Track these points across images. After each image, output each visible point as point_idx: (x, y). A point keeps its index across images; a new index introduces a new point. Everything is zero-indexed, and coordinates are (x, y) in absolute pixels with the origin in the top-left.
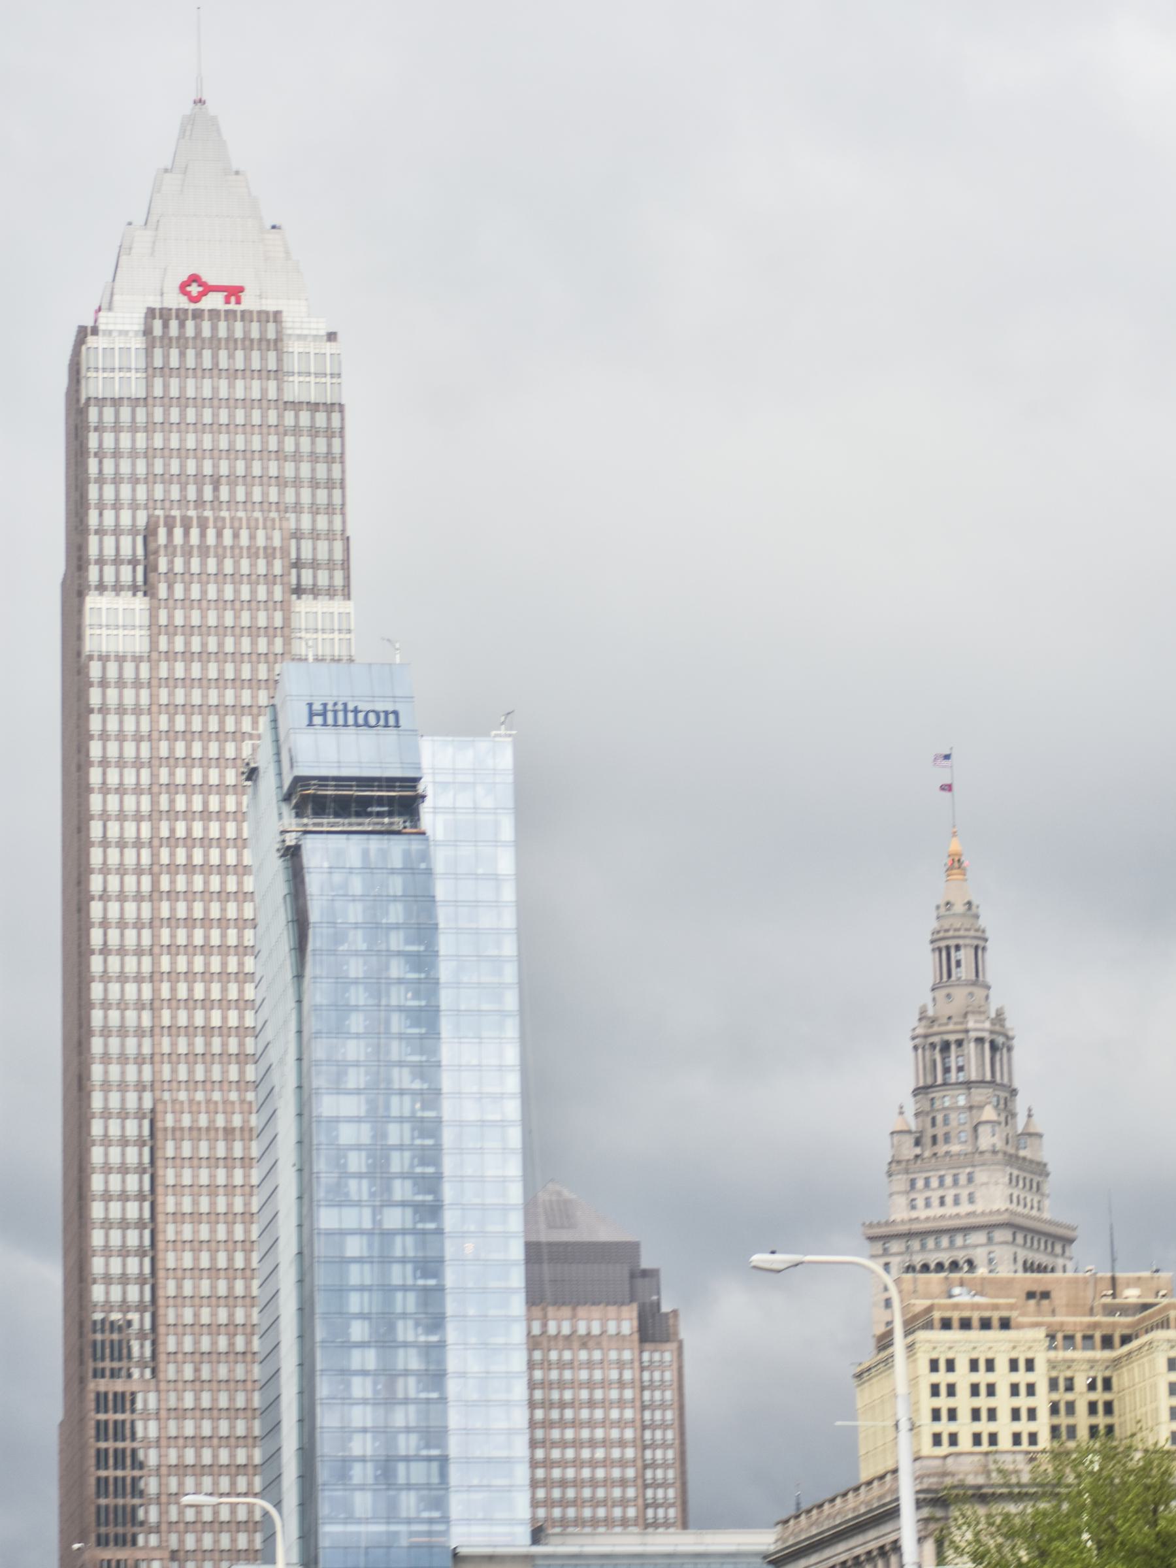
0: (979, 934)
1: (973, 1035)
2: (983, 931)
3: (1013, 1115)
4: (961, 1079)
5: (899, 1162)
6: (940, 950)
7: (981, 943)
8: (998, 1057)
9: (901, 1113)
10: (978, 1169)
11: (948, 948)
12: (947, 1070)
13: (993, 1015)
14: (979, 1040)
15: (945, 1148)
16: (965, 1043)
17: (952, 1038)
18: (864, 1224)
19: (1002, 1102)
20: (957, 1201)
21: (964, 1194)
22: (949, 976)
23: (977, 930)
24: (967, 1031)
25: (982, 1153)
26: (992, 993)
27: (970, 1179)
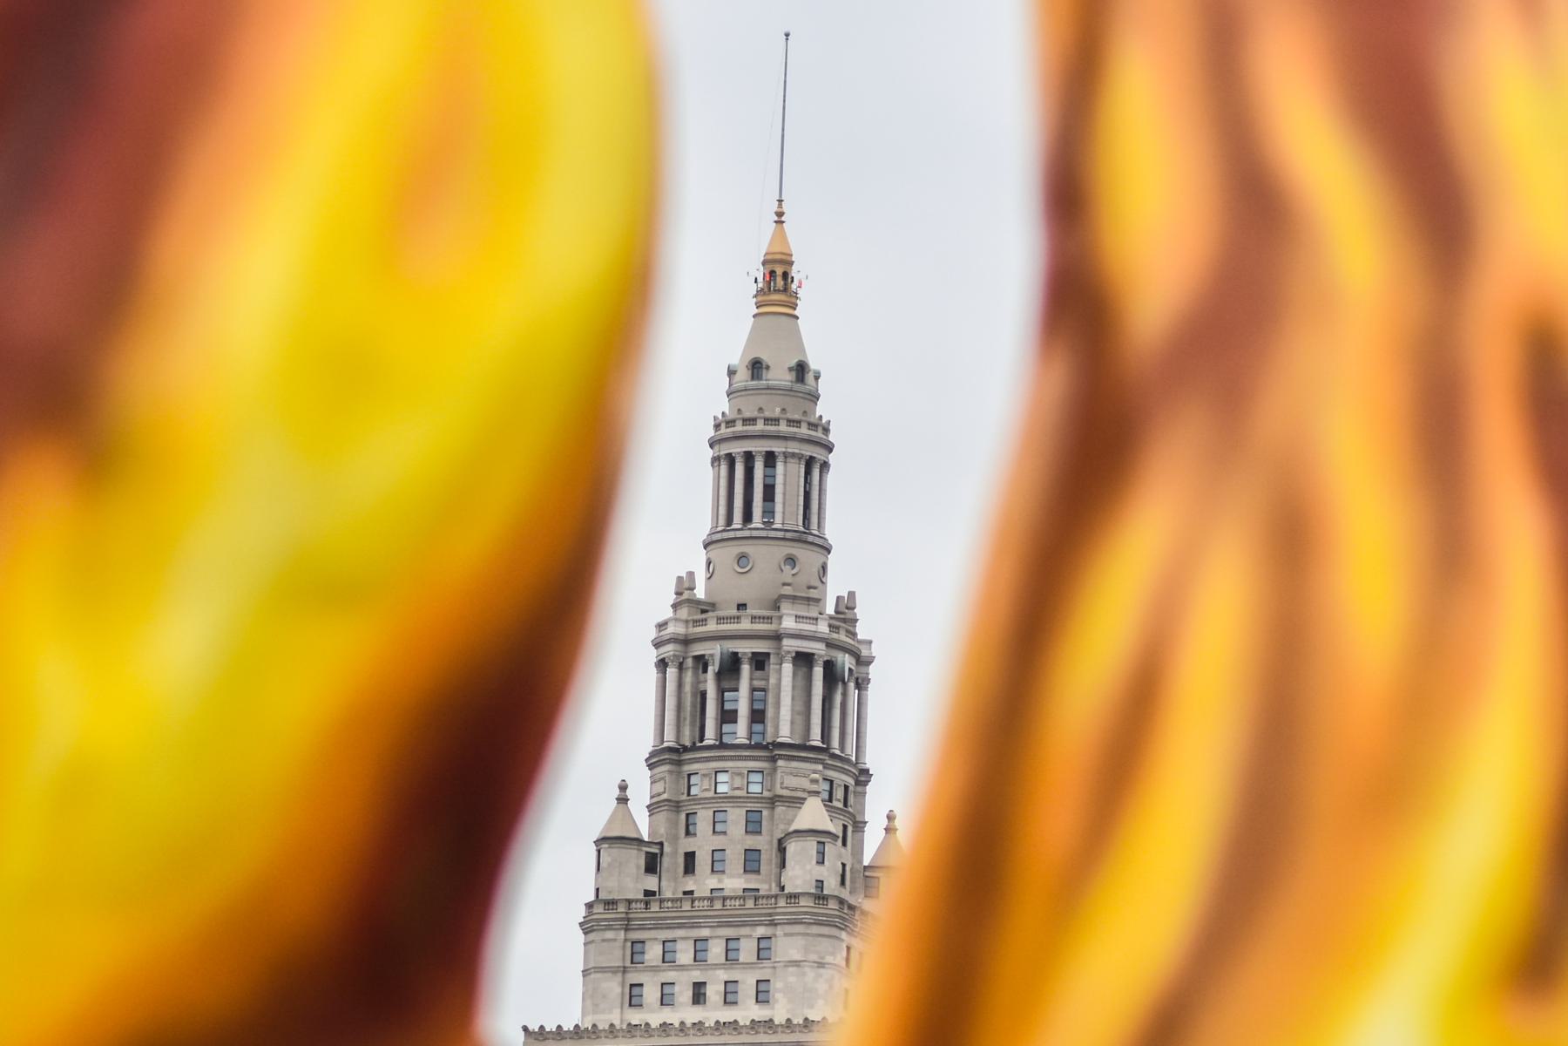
0: (819, 434)
1: (790, 645)
2: (826, 430)
3: (859, 826)
4: (756, 739)
5: (610, 904)
6: (731, 460)
7: (818, 453)
8: (838, 698)
9: (623, 800)
10: (779, 931)
11: (749, 457)
12: (727, 717)
13: (830, 609)
14: (804, 660)
15: (713, 882)
16: (772, 666)
17: (745, 648)
18: (525, 1029)
19: (839, 794)
20: (729, 998)
21: (748, 981)
22: (748, 517)
23: (813, 426)
24: (777, 637)
25: (794, 897)
26: (832, 560)
27: (762, 953)
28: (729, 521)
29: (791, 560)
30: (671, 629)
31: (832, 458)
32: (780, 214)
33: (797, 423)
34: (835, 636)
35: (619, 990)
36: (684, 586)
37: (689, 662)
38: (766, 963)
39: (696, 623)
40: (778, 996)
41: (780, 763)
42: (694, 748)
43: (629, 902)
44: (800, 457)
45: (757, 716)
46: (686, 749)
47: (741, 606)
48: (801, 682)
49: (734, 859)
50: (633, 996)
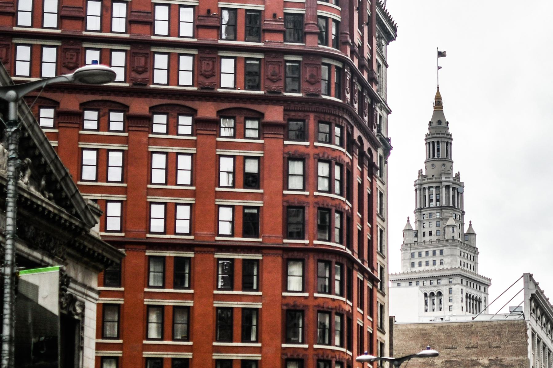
0: (449, 137)
2: (451, 135)
3: (463, 224)
4: (438, 205)
5: (407, 244)
7: (449, 141)
9: (408, 221)
11: (433, 142)
12: (431, 201)
13: (454, 176)
14: (447, 187)
20: (434, 264)
22: (434, 156)
24: (441, 182)
25: (447, 240)
26: (454, 165)
28: (430, 157)
30: (417, 182)
31: (453, 142)
32: (438, 88)
33: (444, 134)
36: (420, 172)
39: (423, 180)
42: (424, 208)
43: (411, 244)
45: (438, 200)
47: (433, 176)
50: (413, 265)
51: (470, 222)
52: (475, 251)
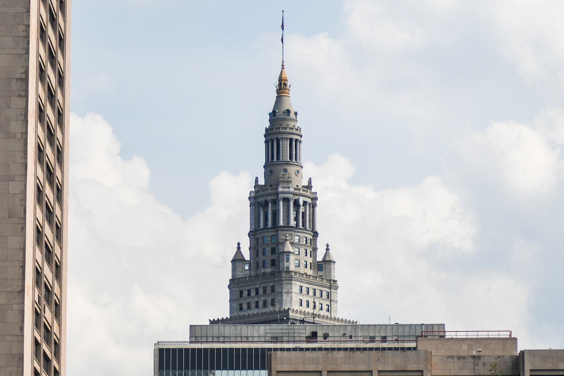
3: (315, 249)
9: (239, 248)
14: (286, 200)
15: (263, 271)
17: (269, 198)
18: (210, 320)
21: (269, 300)
29: (286, 170)
31: (302, 139)
32: (283, 66)
34: (296, 192)
35: (236, 306)
37: (256, 204)
38: (273, 294)
40: (276, 303)
41: (279, 232)
42: (258, 230)
44: (287, 138)
46: (256, 231)
48: (286, 207)
49: (268, 263)
51: (327, 246)
52: (332, 284)
